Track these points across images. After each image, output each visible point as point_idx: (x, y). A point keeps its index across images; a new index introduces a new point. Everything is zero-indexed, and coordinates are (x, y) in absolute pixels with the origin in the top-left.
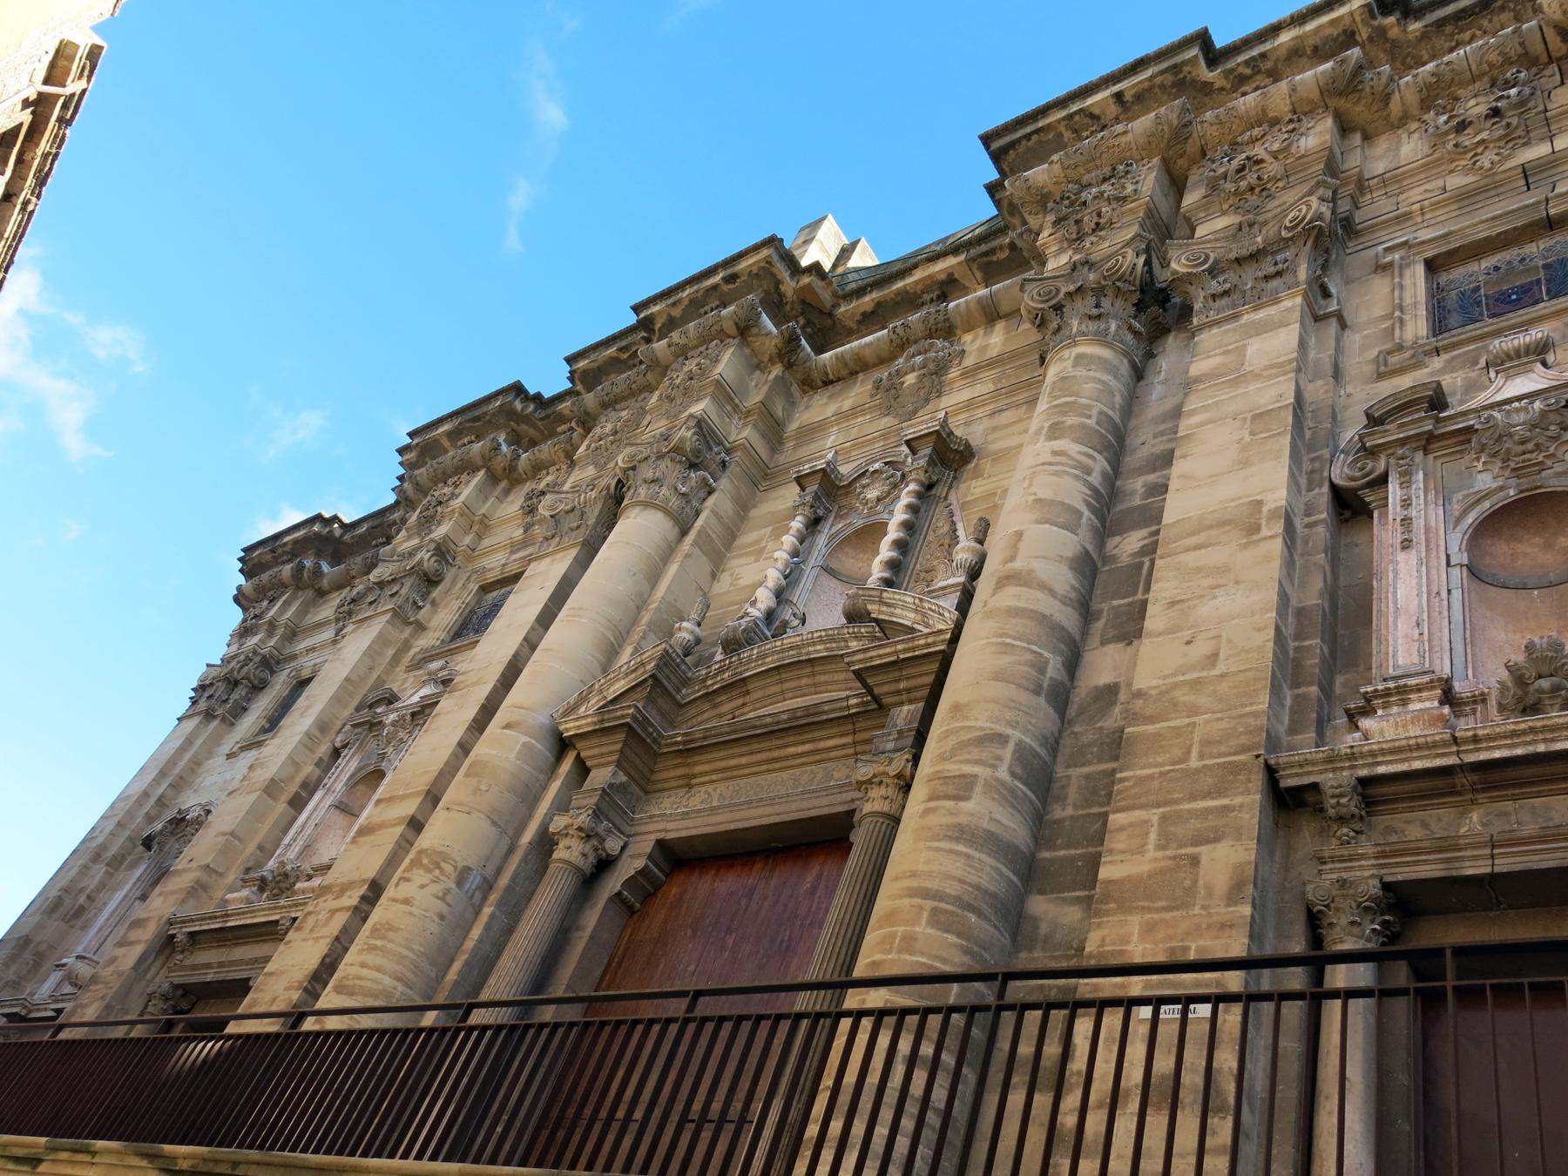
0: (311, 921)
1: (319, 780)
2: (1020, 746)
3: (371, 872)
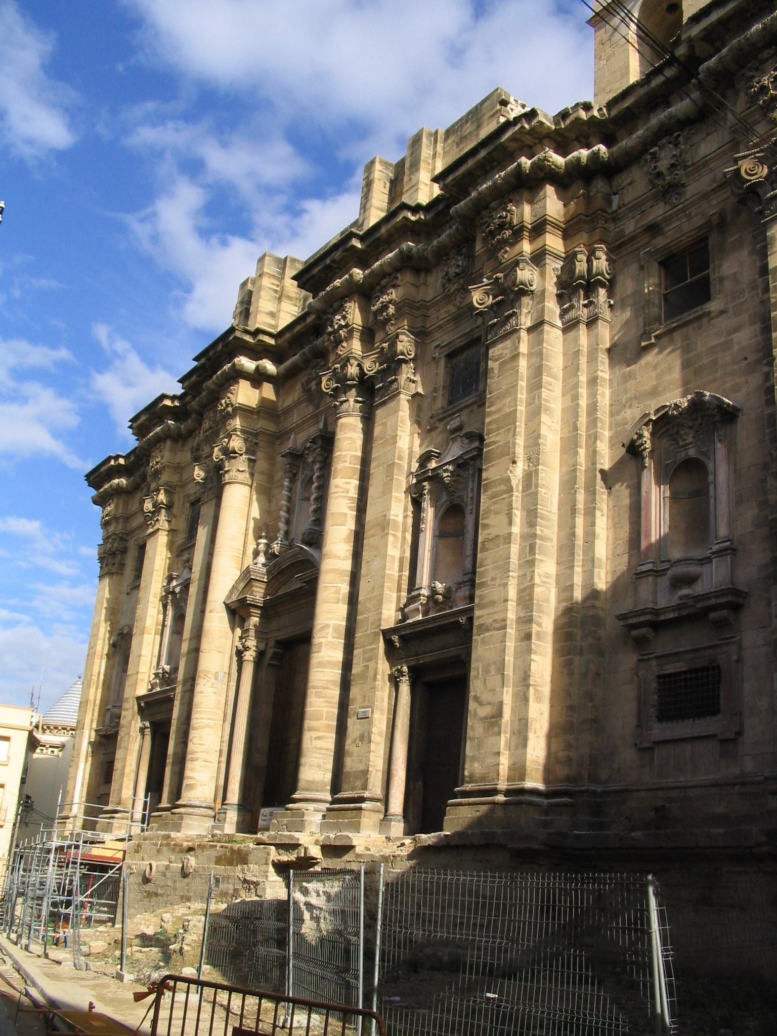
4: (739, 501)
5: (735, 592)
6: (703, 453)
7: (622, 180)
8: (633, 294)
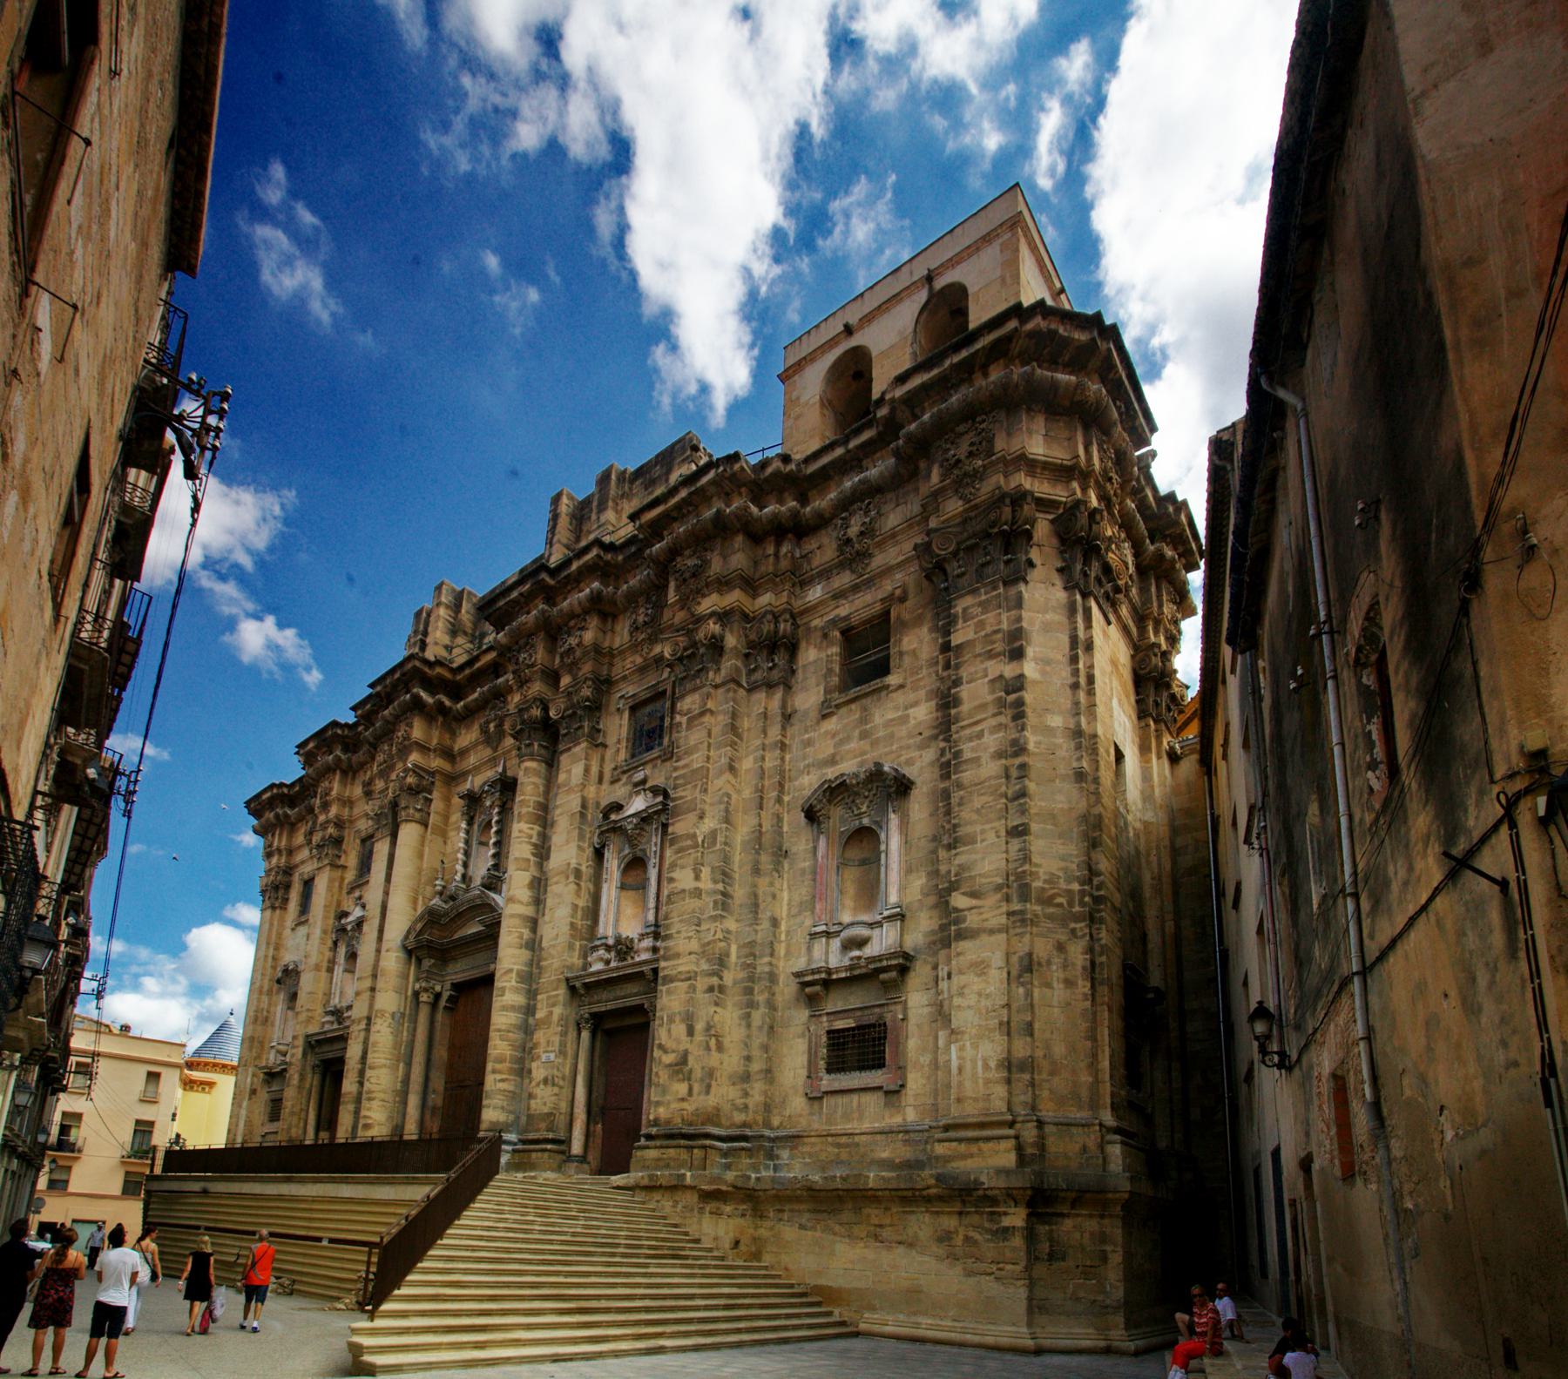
0: (353, 1036)
1: (334, 957)
2: (518, 971)
3: (365, 1014)
4: (909, 870)
5: (907, 956)
6: (876, 823)
7: (811, 544)
8: (815, 661)
